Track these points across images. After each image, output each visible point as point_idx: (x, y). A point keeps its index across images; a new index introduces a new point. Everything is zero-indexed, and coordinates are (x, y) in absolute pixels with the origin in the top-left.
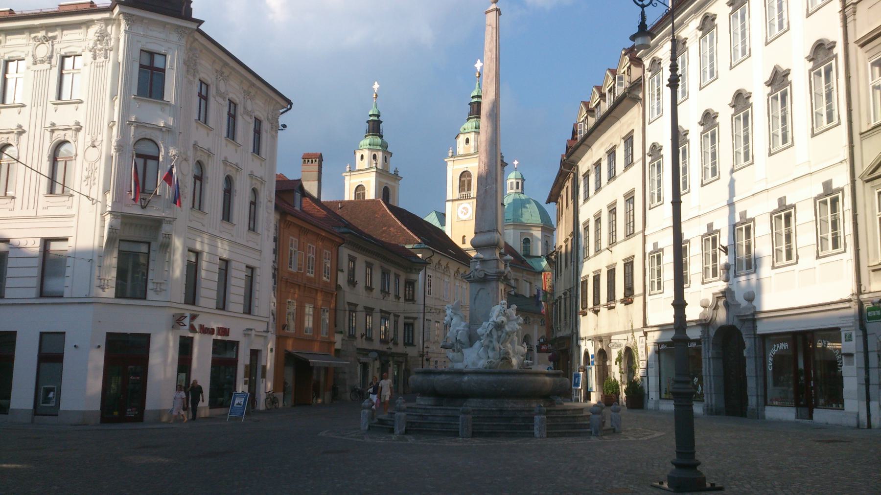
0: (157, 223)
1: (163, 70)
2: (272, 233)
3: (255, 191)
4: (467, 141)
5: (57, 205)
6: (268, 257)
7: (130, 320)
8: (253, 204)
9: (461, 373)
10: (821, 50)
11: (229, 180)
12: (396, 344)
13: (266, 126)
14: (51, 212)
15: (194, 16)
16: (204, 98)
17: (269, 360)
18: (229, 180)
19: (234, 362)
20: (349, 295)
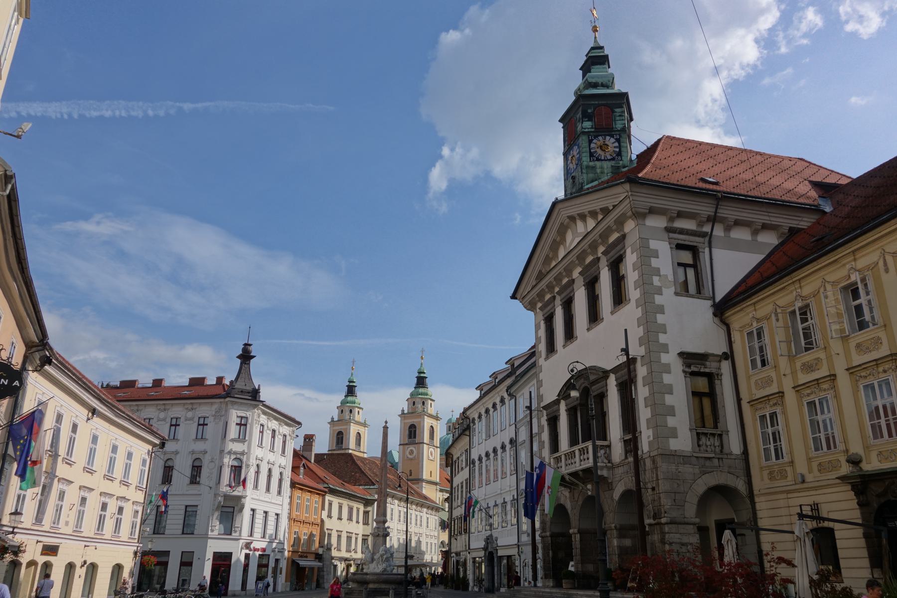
0: (239, 498)
1: (246, 425)
2: (289, 494)
3: (281, 473)
4: (414, 403)
5: (194, 489)
6: (286, 507)
7: (223, 546)
8: (280, 481)
9: (367, 574)
10: (512, 441)
11: (270, 470)
12: (356, 552)
13: (288, 438)
14: (190, 492)
15: (261, 399)
16: (262, 432)
17: (283, 565)
18: (270, 470)
19: (267, 566)
20: (328, 524)
